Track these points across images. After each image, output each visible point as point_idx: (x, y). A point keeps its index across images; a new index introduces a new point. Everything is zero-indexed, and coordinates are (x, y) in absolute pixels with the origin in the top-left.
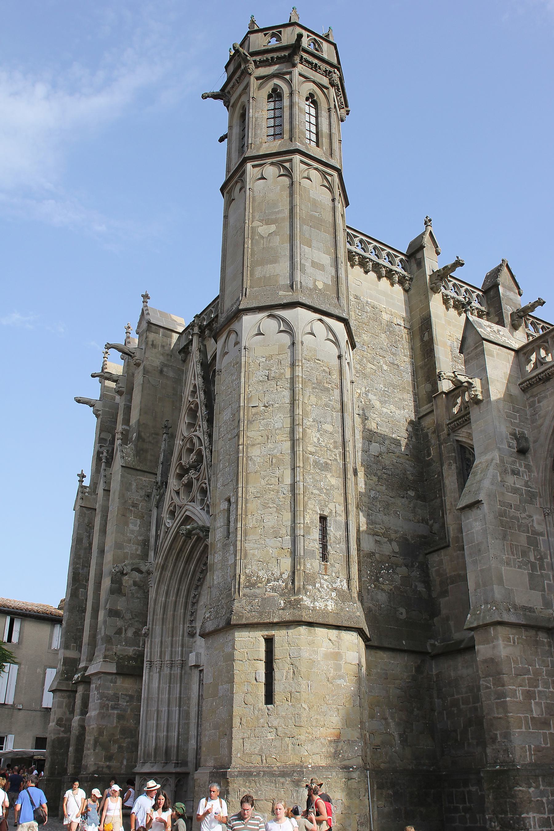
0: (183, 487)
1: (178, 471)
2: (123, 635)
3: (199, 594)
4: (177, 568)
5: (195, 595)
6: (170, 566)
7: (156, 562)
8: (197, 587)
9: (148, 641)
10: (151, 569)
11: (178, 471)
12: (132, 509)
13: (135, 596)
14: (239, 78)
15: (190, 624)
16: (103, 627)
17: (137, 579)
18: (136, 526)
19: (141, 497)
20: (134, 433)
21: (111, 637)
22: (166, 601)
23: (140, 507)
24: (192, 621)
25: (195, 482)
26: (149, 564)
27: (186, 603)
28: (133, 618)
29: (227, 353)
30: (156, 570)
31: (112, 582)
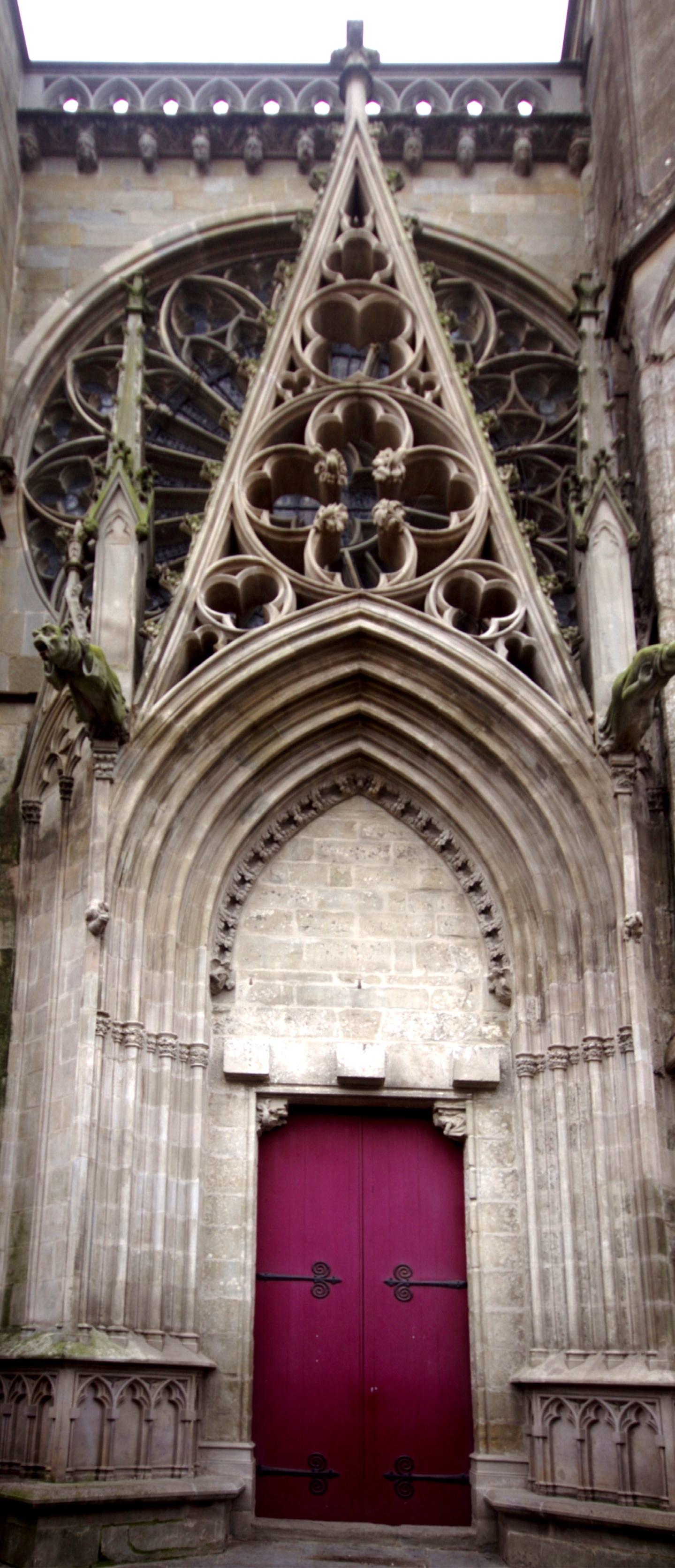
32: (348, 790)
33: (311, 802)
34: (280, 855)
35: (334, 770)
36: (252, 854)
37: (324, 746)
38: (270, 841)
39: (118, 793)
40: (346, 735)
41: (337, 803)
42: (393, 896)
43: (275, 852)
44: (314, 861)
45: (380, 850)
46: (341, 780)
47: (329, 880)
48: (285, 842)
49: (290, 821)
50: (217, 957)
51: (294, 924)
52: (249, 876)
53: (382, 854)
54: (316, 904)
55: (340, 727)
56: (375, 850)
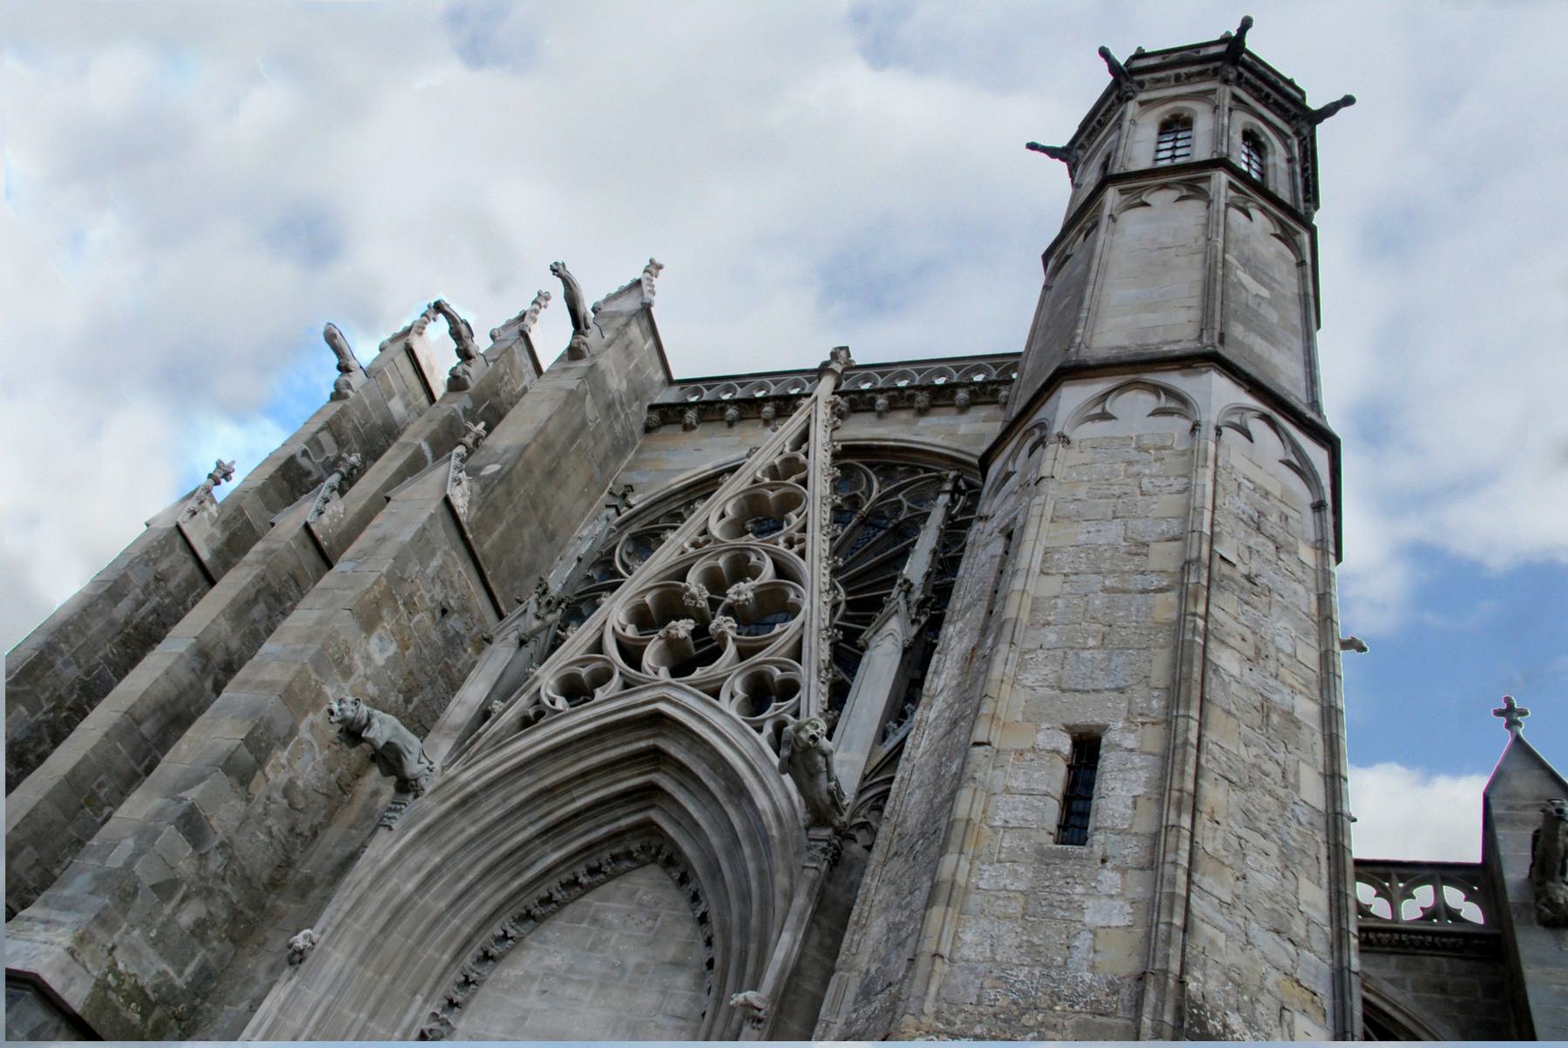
0: (661, 643)
1: (648, 599)
2: (168, 909)
3: (518, 941)
4: (504, 828)
5: (505, 937)
6: (491, 810)
7: (451, 772)
8: (528, 916)
9: (290, 979)
10: (423, 781)
11: (648, 599)
12: (402, 608)
13: (269, 822)
14: (1189, 76)
15: (444, 1010)
16: (129, 844)
17: (300, 783)
18: (382, 650)
19: (432, 599)
20: (495, 463)
21: (136, 890)
22: (410, 897)
23: (416, 619)
24: (452, 1004)
25: (731, 650)
26: (427, 764)
27: (468, 942)
28: (223, 879)
29: (1105, 416)
30: (434, 792)
31: (246, 741)
32: (642, 857)
33: (601, 866)
34: (557, 915)
35: (628, 836)
36: (524, 912)
37: (620, 812)
38: (549, 900)
39: (392, 840)
40: (642, 804)
41: (629, 870)
42: (639, 966)
43: (553, 913)
44: (584, 925)
45: (648, 918)
46: (635, 846)
47: (588, 945)
48: (566, 904)
49: (575, 882)
50: (438, 1012)
51: (536, 987)
52: (512, 932)
53: (650, 923)
54: (564, 968)
55: (635, 796)
56: (644, 919)
